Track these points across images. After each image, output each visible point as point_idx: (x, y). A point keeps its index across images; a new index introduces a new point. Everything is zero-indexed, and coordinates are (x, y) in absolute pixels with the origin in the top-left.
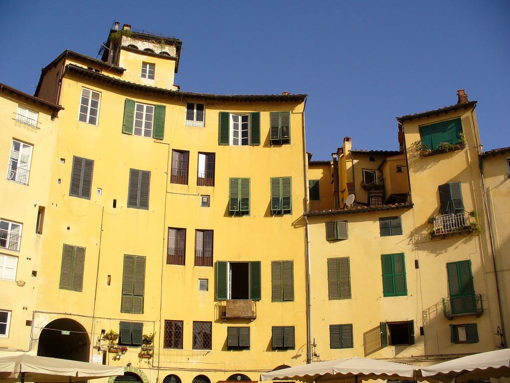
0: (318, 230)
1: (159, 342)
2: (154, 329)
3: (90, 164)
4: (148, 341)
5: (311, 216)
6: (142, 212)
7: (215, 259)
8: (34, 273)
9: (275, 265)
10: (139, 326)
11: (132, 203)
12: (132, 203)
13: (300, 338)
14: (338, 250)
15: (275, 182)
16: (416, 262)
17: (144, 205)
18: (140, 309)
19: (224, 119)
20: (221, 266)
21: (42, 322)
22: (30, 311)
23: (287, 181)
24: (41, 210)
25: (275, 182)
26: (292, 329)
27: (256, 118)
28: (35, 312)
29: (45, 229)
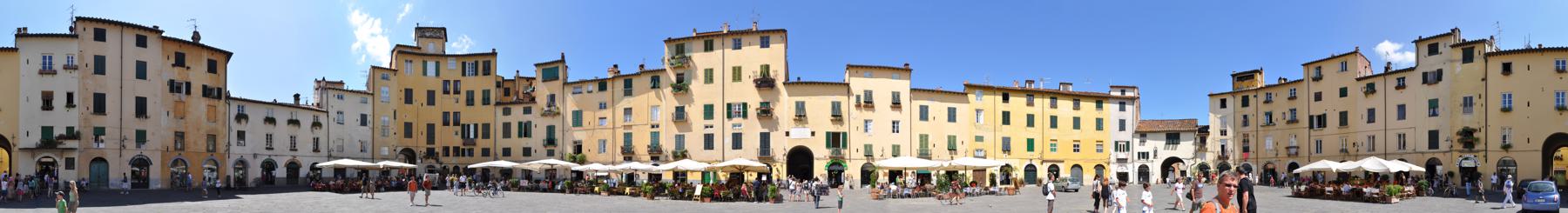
0: (500, 110)
1: (441, 154)
2: (438, 149)
3: (411, 90)
4: (438, 153)
6: (433, 107)
7: (462, 122)
9: (483, 125)
10: (434, 149)
11: (429, 104)
12: (429, 104)
13: (492, 151)
14: (507, 119)
15: (484, 91)
17: (434, 104)
18: (434, 143)
19: (464, 64)
20: (463, 126)
21: (399, 149)
23: (489, 91)
25: (484, 91)
27: (477, 62)
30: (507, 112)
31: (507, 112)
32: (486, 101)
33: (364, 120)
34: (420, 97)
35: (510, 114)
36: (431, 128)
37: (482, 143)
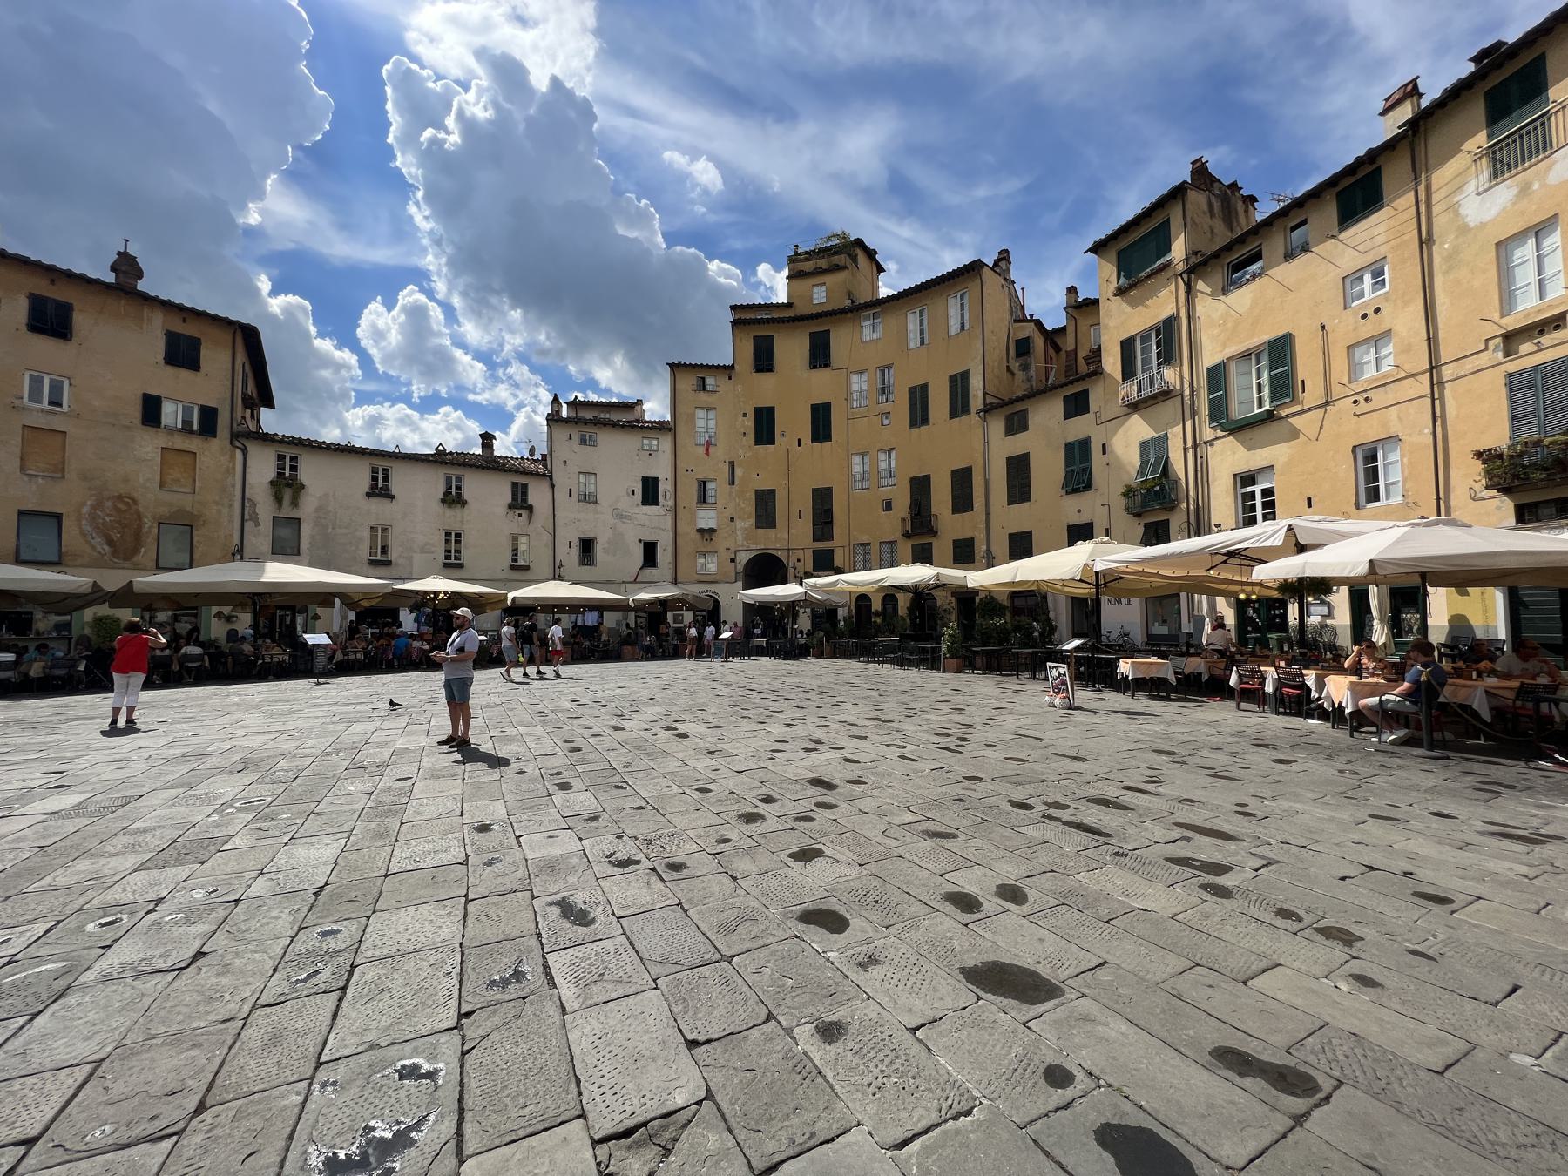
0: (997, 426)
3: (771, 410)
5: (988, 410)
8: (732, 519)
11: (815, 439)
12: (815, 439)
13: (980, 549)
16: (1104, 445)
17: (828, 437)
18: (831, 538)
21: (744, 558)
22: (733, 549)
23: (965, 376)
24: (732, 464)
25: (953, 379)
26: (971, 541)
28: (736, 551)
29: (736, 482)
30: (1016, 425)
31: (1016, 425)
32: (959, 405)
33: (650, 491)
34: (794, 423)
35: (1024, 427)
36: (822, 500)
37: (951, 525)
